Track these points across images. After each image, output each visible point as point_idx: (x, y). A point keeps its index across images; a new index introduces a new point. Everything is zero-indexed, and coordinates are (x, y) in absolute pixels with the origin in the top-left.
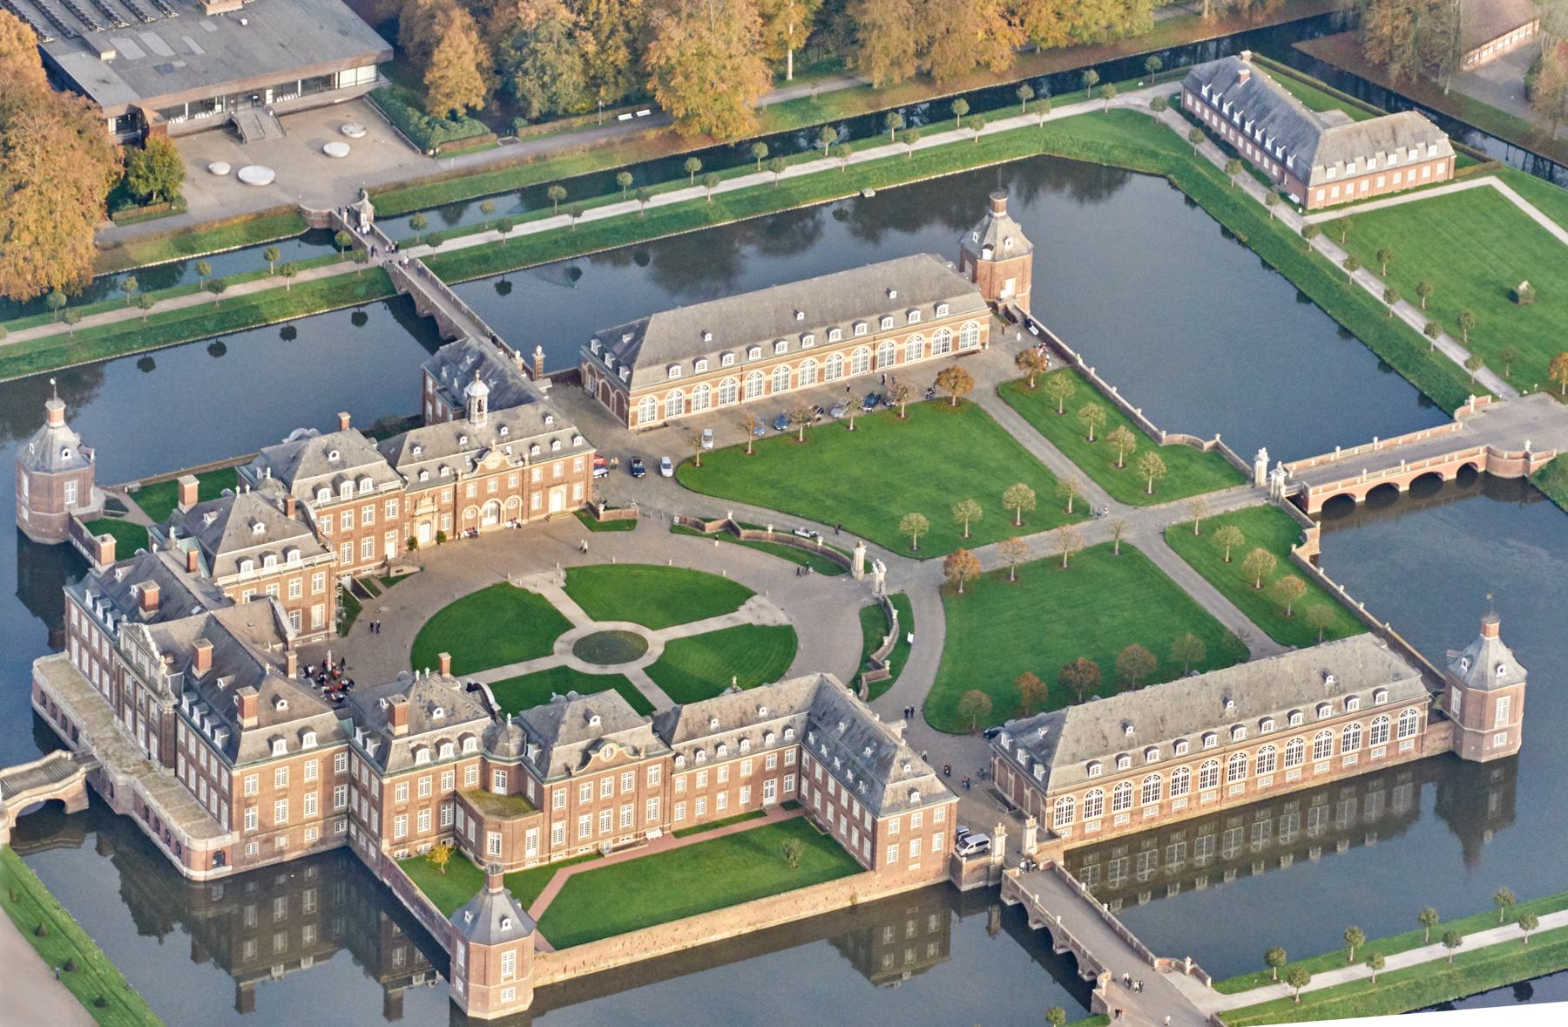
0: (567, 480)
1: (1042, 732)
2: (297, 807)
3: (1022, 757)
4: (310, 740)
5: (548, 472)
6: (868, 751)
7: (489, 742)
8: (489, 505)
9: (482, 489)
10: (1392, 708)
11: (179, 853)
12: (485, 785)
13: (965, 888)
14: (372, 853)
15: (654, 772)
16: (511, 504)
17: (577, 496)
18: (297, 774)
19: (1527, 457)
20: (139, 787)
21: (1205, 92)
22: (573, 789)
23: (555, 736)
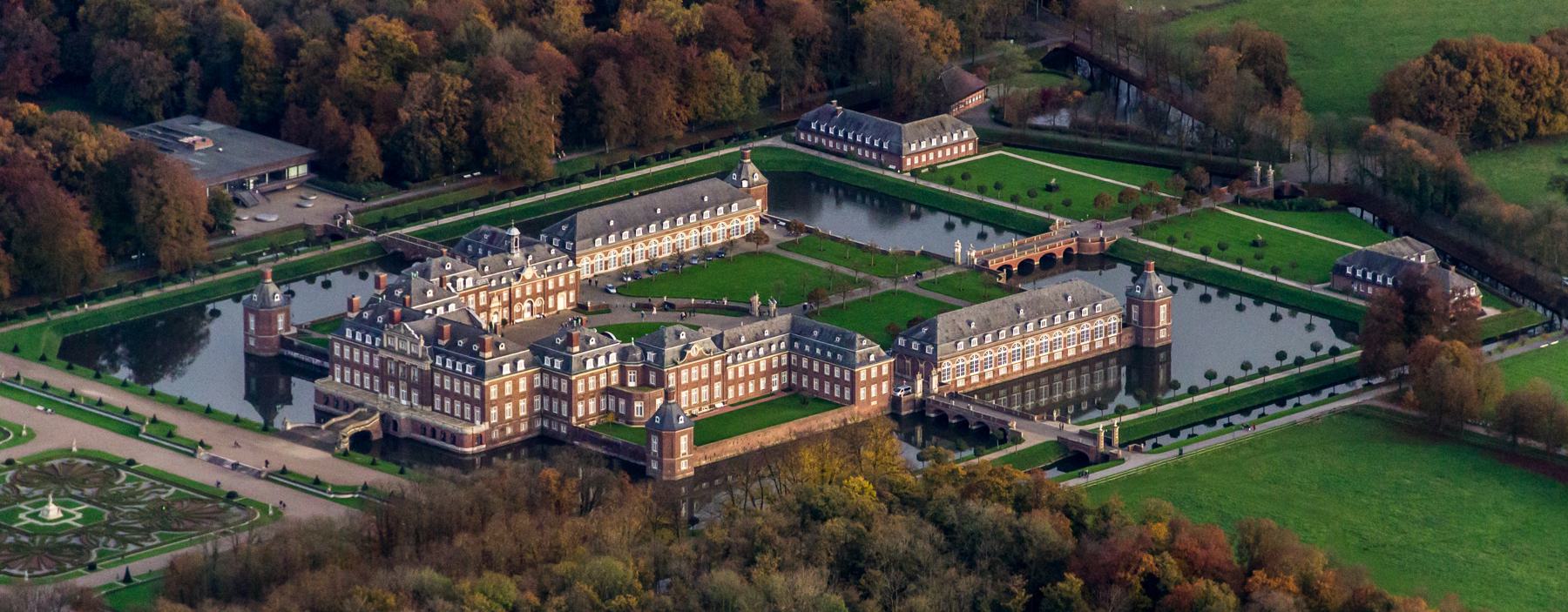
0: (567, 288)
1: (925, 330)
2: (516, 409)
3: (915, 346)
4: (521, 365)
5: (556, 283)
6: (838, 339)
7: (624, 355)
8: (527, 305)
9: (523, 290)
10: (1105, 315)
11: (453, 443)
12: (623, 382)
13: (904, 413)
14: (564, 430)
15: (718, 365)
16: (537, 304)
17: (572, 300)
18: (516, 386)
19: (1102, 240)
20: (416, 416)
21: (813, 127)
22: (678, 372)
23: (663, 345)
